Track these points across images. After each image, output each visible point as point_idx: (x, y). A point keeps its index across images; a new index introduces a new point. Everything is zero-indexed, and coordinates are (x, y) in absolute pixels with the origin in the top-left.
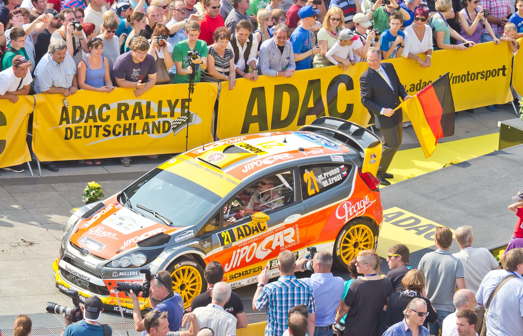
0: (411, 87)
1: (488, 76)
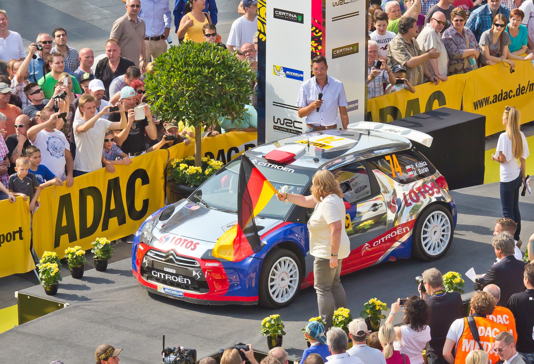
0: (494, 98)
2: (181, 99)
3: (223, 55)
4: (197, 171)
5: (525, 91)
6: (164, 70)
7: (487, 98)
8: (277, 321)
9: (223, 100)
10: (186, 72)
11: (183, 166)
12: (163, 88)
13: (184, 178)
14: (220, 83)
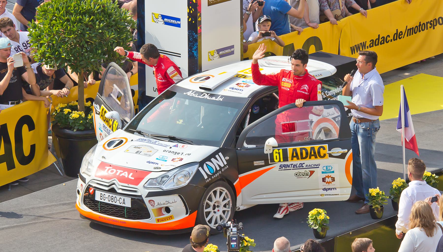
1: (435, 24)
2: (63, 46)
3: (104, 4)
4: (80, 115)
6: (47, 19)
7: (364, 42)
9: (104, 47)
10: (68, 20)
12: (45, 36)
13: (67, 122)
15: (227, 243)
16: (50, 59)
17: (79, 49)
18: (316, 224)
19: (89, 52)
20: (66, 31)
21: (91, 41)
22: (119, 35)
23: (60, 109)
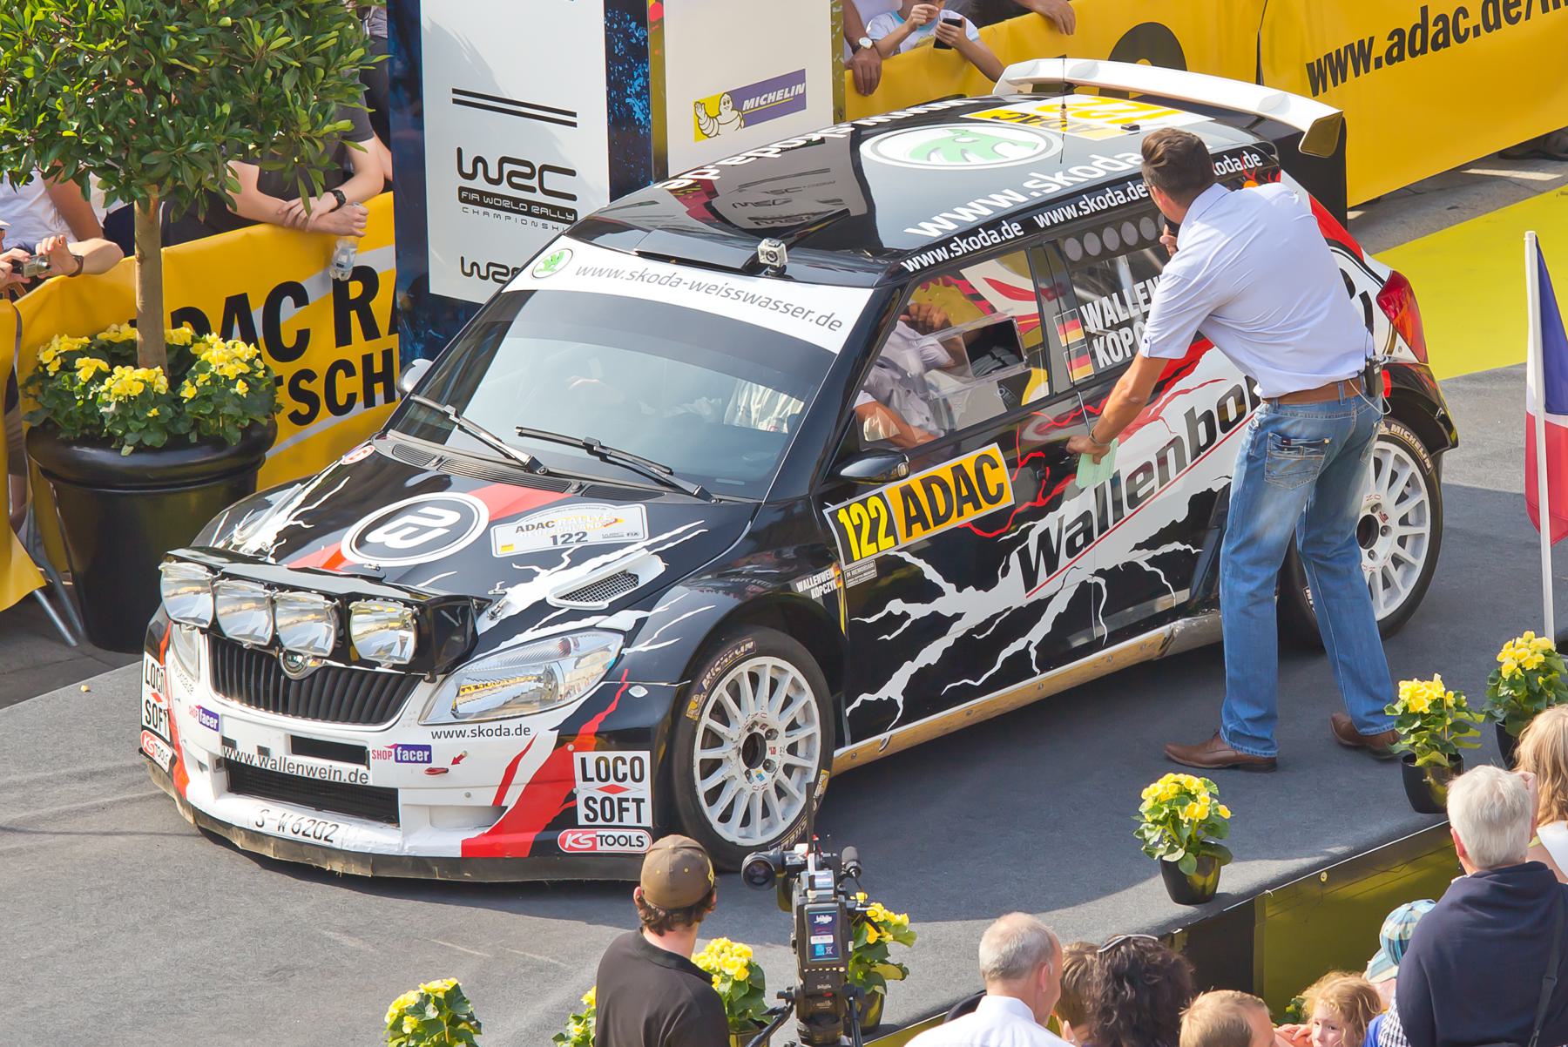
0: (1392, 42)
2: (66, 89)
4: (148, 386)
5: (1523, 9)
7: (1361, 43)
8: (449, 1007)
11: (86, 368)
14: (229, 19)
15: (793, 937)
16: (12, 147)
17: (136, 99)
18: (1172, 842)
19: (179, 114)
20: (78, 22)
21: (186, 63)
22: (307, 38)
23: (59, 358)
